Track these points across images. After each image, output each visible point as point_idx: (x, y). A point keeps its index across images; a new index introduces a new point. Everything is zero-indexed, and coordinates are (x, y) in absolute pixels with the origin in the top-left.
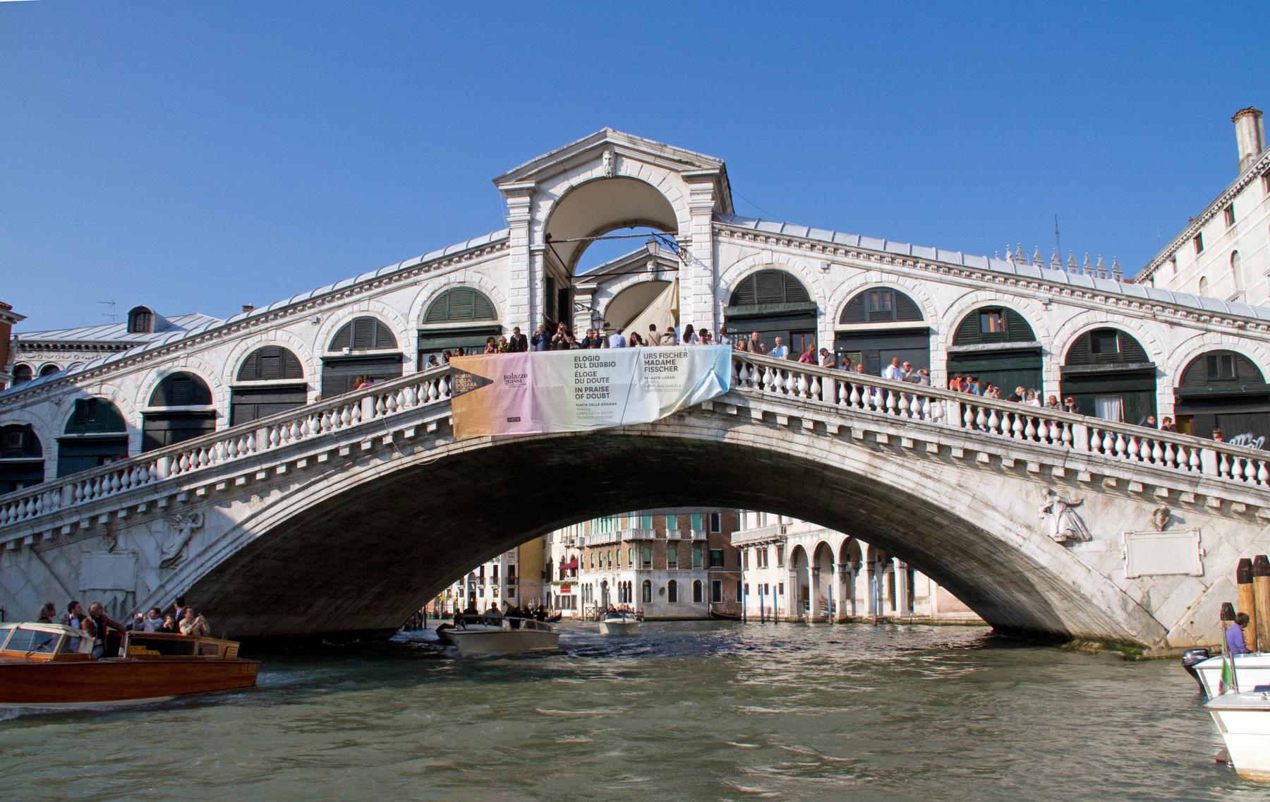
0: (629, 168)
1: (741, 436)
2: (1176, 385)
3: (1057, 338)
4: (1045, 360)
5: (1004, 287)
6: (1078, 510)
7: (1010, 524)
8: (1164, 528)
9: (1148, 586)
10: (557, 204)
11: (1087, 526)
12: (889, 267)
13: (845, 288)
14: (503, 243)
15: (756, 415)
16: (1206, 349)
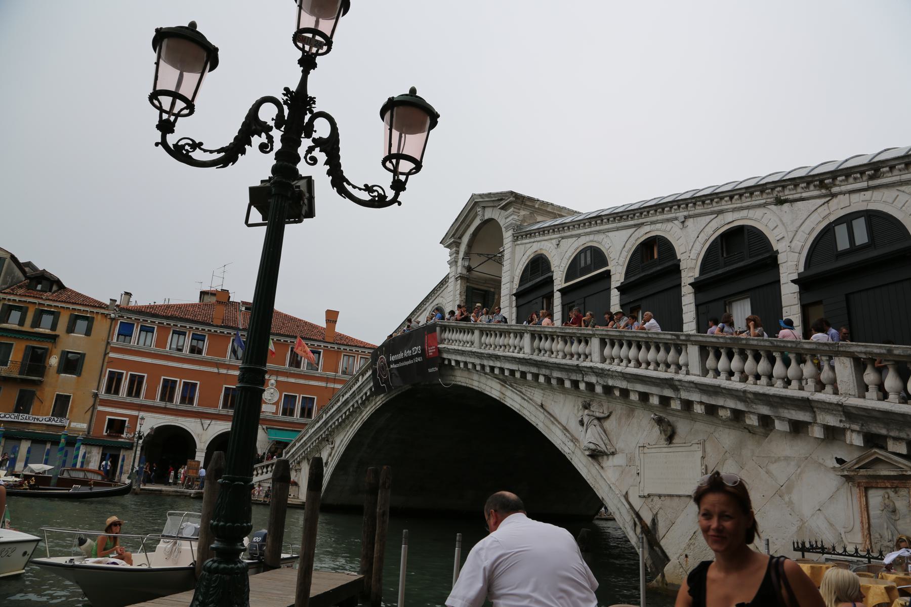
0: (489, 214)
1: (458, 379)
2: (801, 269)
3: (693, 251)
4: (683, 274)
5: (654, 218)
6: (607, 424)
7: (564, 439)
8: (670, 439)
9: (657, 507)
10: (470, 245)
11: (614, 441)
12: (588, 230)
13: (567, 255)
14: (447, 277)
15: (453, 363)
16: (832, 218)
